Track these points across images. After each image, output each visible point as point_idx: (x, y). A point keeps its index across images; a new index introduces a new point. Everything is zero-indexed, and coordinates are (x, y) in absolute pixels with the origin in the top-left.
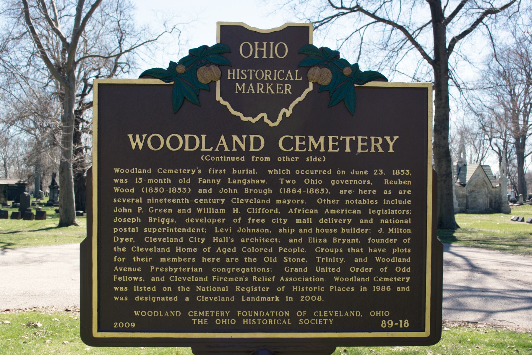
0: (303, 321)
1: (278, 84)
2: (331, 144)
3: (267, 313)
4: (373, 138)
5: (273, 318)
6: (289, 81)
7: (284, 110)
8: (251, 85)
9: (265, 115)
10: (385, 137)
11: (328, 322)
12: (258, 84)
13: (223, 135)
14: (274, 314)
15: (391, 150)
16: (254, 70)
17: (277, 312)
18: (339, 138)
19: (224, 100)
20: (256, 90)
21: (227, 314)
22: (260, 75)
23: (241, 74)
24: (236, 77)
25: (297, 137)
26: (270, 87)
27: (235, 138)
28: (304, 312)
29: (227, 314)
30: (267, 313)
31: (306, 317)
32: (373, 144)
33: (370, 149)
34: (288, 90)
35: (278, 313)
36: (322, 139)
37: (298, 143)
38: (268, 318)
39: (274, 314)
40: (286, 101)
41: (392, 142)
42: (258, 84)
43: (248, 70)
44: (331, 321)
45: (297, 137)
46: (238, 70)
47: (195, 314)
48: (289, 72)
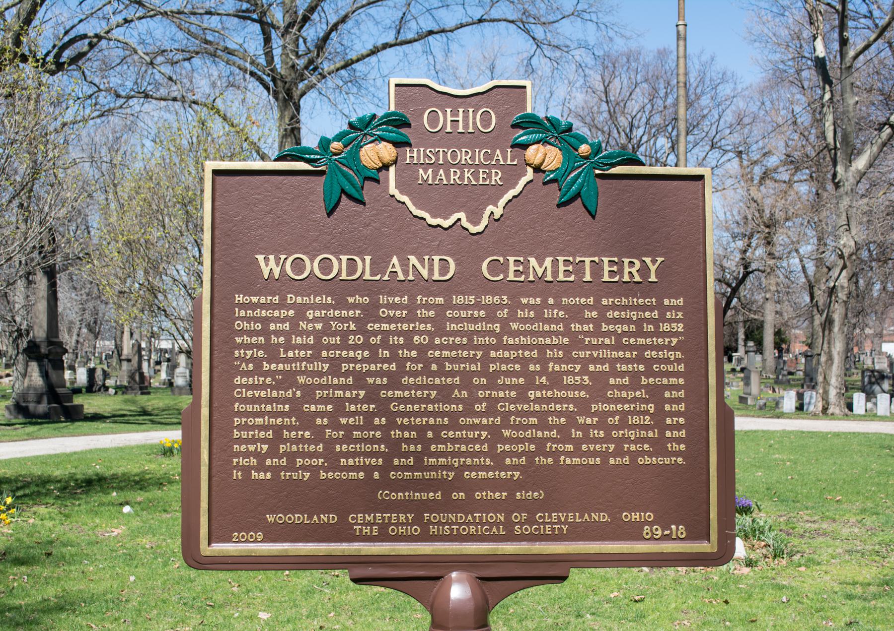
0: (521, 529)
1: (481, 171)
2: (562, 268)
3: (470, 517)
4: (626, 261)
5: (476, 524)
6: (497, 166)
7: (490, 208)
8: (441, 172)
9: (462, 215)
10: (643, 259)
11: (560, 529)
12: (452, 170)
13: (395, 257)
14: (481, 518)
15: (653, 278)
16: (446, 150)
17: (484, 515)
18: (574, 259)
19: (401, 193)
20: (448, 178)
21: (410, 518)
22: (454, 156)
23: (426, 156)
24: (419, 158)
25: (512, 259)
26: (469, 175)
27: (413, 260)
28: (523, 514)
29: (410, 518)
30: (470, 517)
31: (527, 522)
32: (627, 270)
33: (622, 277)
34: (496, 178)
35: (487, 516)
36: (548, 261)
37: (512, 268)
38: (468, 524)
39: (481, 518)
40: (493, 193)
41: (654, 265)
42: (452, 170)
43: (437, 150)
44: (565, 529)
45: (512, 259)
46: (422, 150)
47: (359, 519)
48: (498, 152)
